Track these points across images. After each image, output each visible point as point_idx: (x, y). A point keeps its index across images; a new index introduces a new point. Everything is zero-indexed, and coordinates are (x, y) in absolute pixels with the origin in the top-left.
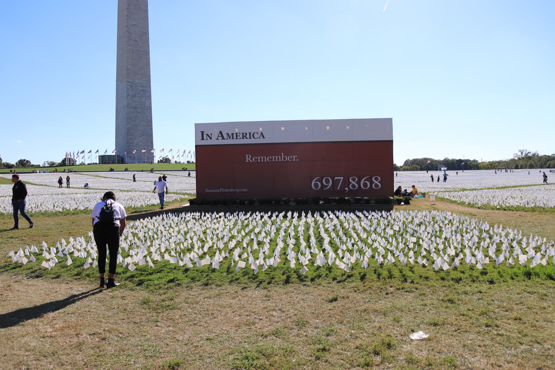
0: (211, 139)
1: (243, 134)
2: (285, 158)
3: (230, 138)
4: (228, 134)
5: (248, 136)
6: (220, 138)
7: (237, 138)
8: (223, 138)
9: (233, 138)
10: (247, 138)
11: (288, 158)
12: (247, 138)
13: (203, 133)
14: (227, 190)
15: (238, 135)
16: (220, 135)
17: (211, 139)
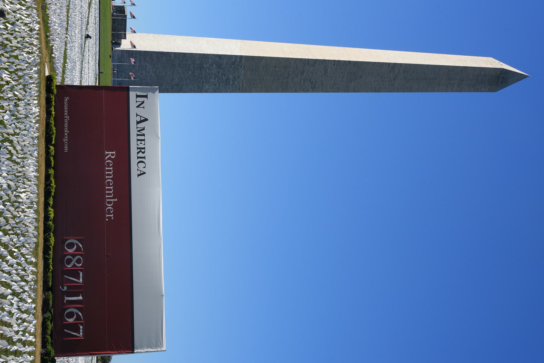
0: (138, 107)
1: (144, 148)
2: (110, 203)
3: (139, 131)
4: (144, 129)
5: (141, 155)
6: (139, 119)
7: (138, 140)
8: (138, 123)
9: (138, 135)
10: (138, 153)
11: (110, 207)
12: (138, 153)
13: (146, 96)
14: (66, 125)
15: (143, 142)
16: (142, 119)
17: (138, 107)
